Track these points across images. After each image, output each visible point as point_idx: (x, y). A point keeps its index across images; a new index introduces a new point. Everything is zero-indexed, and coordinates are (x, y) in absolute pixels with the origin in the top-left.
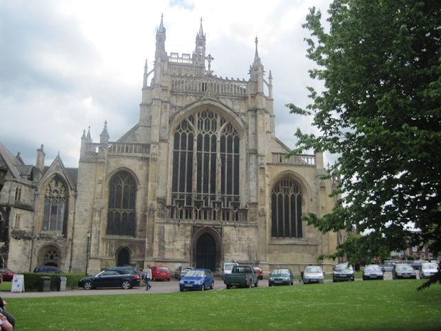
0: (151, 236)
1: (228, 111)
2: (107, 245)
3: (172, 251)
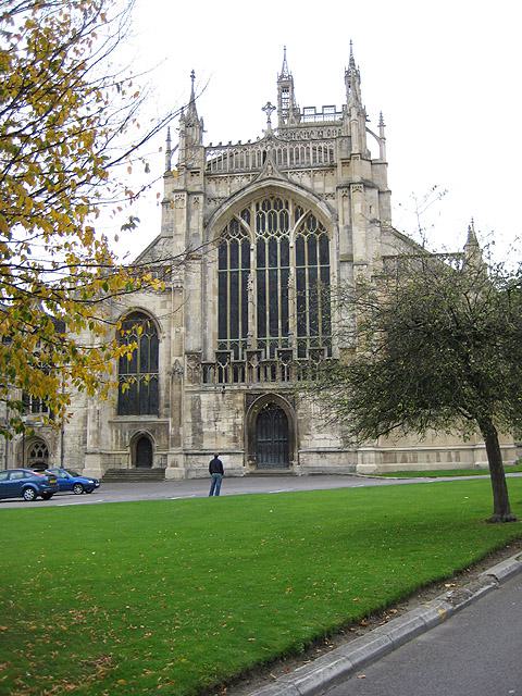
0: (176, 414)
1: (303, 193)
2: (117, 432)
3: (214, 435)
